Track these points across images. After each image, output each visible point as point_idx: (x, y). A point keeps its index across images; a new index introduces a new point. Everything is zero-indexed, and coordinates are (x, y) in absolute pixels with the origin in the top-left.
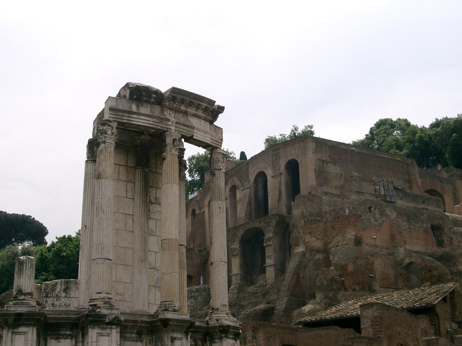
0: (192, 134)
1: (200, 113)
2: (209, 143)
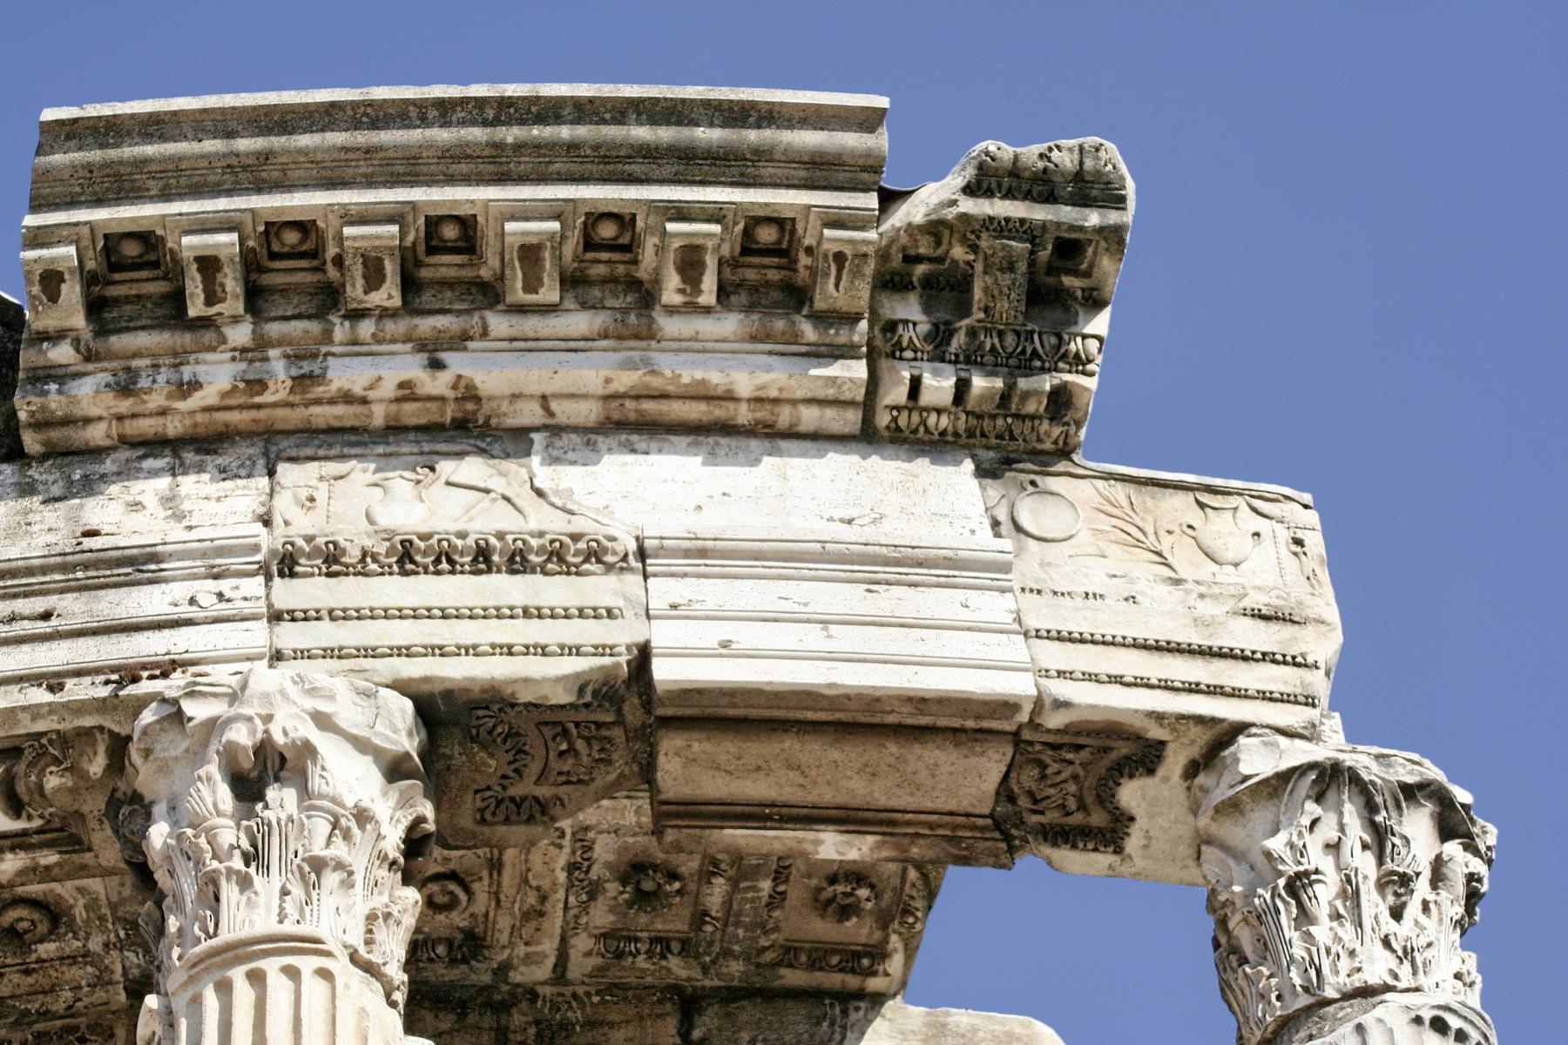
0: (623, 634)
1: (714, 353)
2: (1021, 686)
